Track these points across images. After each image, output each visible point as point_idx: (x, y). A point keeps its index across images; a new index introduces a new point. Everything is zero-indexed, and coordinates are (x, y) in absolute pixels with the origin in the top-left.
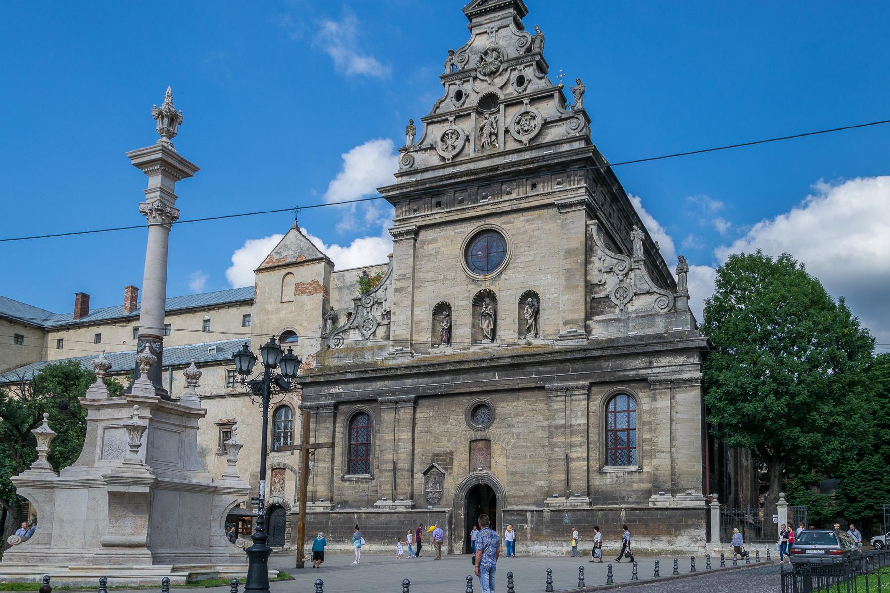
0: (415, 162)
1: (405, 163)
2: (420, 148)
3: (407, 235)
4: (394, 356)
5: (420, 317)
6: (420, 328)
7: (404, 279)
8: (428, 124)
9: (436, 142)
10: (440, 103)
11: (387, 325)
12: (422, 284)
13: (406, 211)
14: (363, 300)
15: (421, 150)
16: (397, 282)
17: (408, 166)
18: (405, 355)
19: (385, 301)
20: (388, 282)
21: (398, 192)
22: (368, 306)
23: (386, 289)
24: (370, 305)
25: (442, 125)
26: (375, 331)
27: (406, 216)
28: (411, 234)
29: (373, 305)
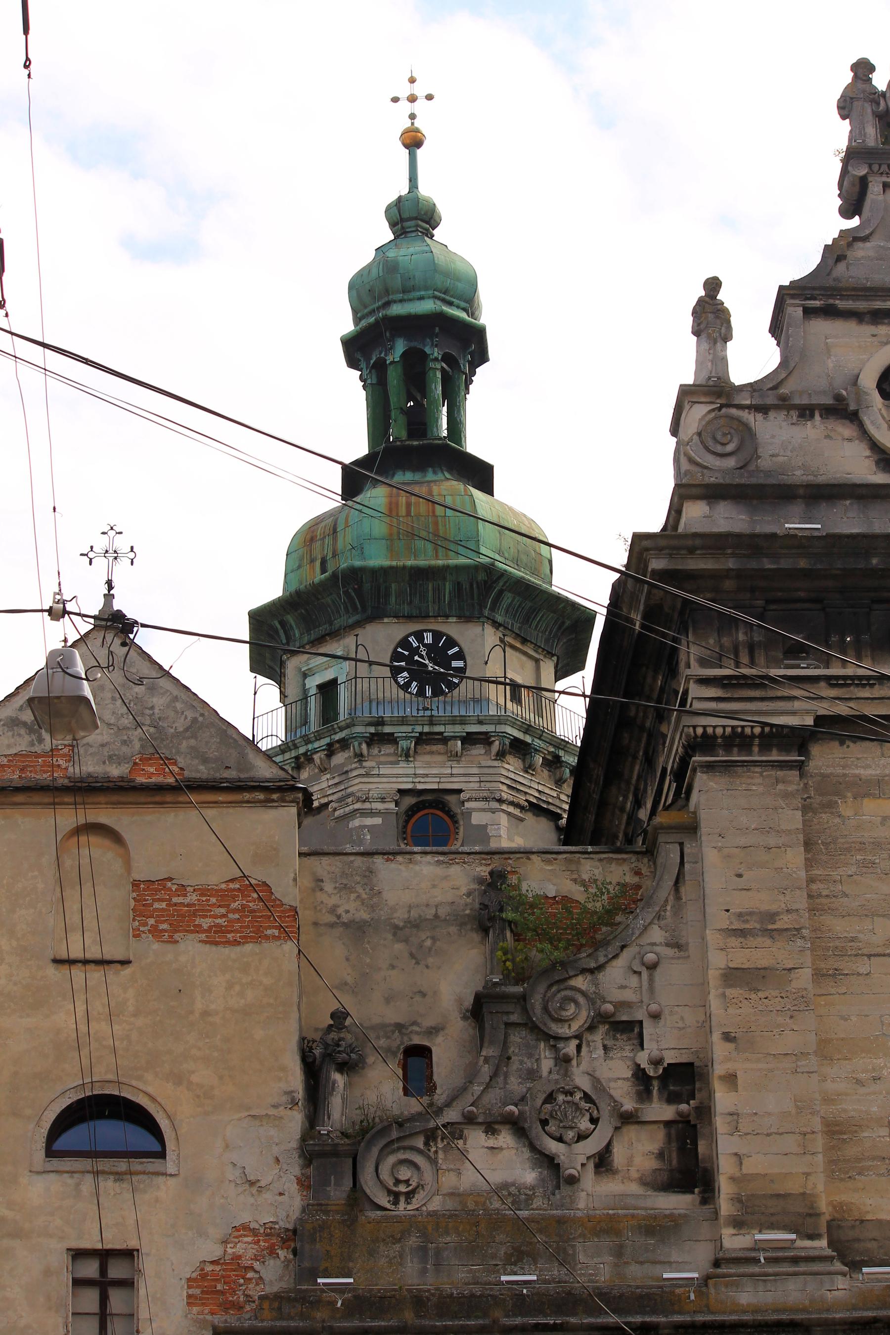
0: (760, 450)
1: (719, 449)
2: (784, 398)
3: (765, 747)
4: (756, 1269)
5: (851, 1108)
6: (851, 1151)
7: (771, 934)
8: (808, 312)
9: (859, 394)
10: (849, 245)
11: (668, 1124)
12: (847, 965)
13: (752, 649)
14: (536, 1001)
15: (784, 404)
16: (734, 942)
17: (731, 462)
18: (802, 1268)
19: (656, 1016)
20: (657, 934)
21: (731, 564)
22: (563, 1030)
23: (652, 967)
24: (575, 1026)
25: (869, 329)
26: (608, 1148)
27: (752, 663)
28: (784, 748)
29: (591, 1028)
